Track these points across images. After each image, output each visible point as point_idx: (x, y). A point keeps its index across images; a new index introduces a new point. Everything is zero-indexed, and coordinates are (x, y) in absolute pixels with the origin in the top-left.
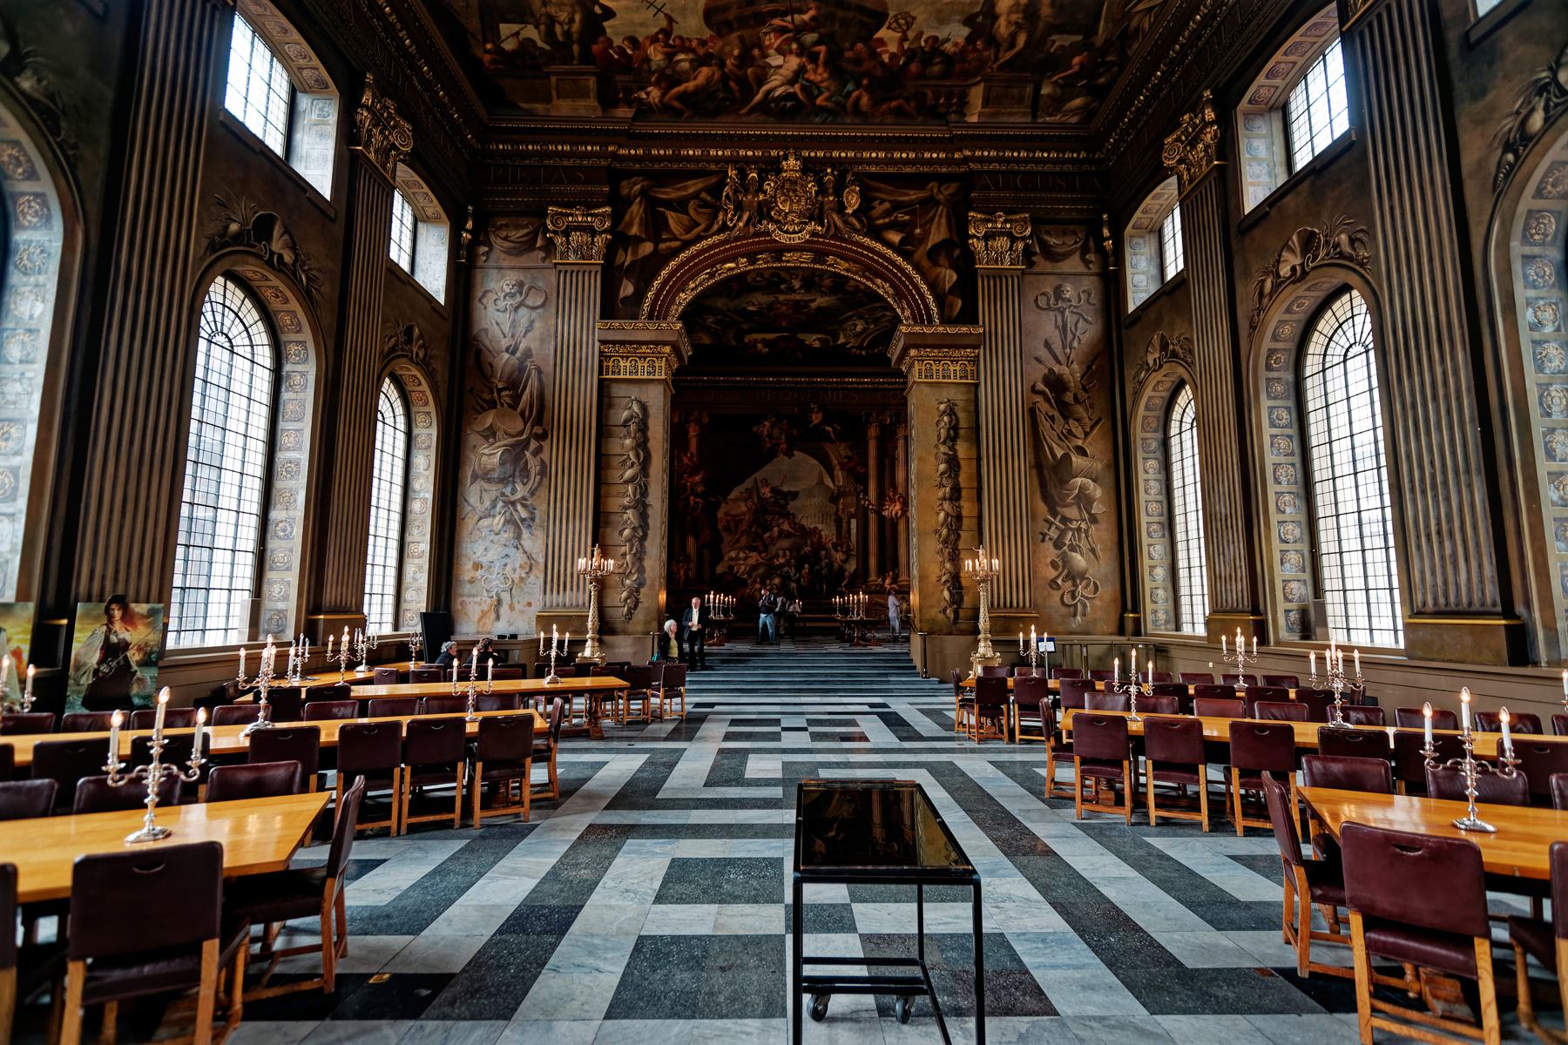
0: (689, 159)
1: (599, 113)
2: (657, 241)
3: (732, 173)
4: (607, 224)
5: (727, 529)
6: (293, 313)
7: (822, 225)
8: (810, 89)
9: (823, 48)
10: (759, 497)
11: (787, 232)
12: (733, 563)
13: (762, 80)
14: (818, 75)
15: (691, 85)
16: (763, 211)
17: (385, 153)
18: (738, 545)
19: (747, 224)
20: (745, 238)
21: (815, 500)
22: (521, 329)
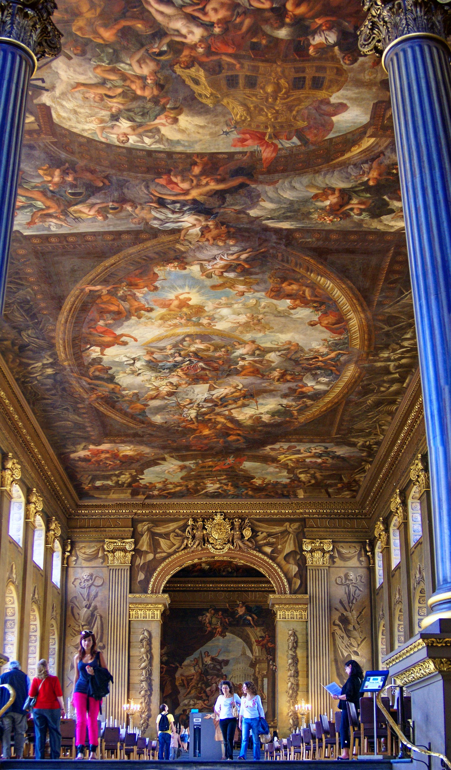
0: (170, 514)
1: (130, 497)
2: (155, 553)
3: (190, 522)
4: (133, 547)
5: (183, 685)
6: (35, 615)
7: (233, 545)
8: (225, 491)
9: (230, 484)
10: (203, 664)
11: (217, 549)
12: (186, 708)
13: (203, 489)
14: (229, 488)
15: (173, 491)
16: (205, 540)
17: (54, 541)
18: (190, 696)
19: (198, 545)
20: (197, 551)
21: (241, 666)
22: (91, 596)
